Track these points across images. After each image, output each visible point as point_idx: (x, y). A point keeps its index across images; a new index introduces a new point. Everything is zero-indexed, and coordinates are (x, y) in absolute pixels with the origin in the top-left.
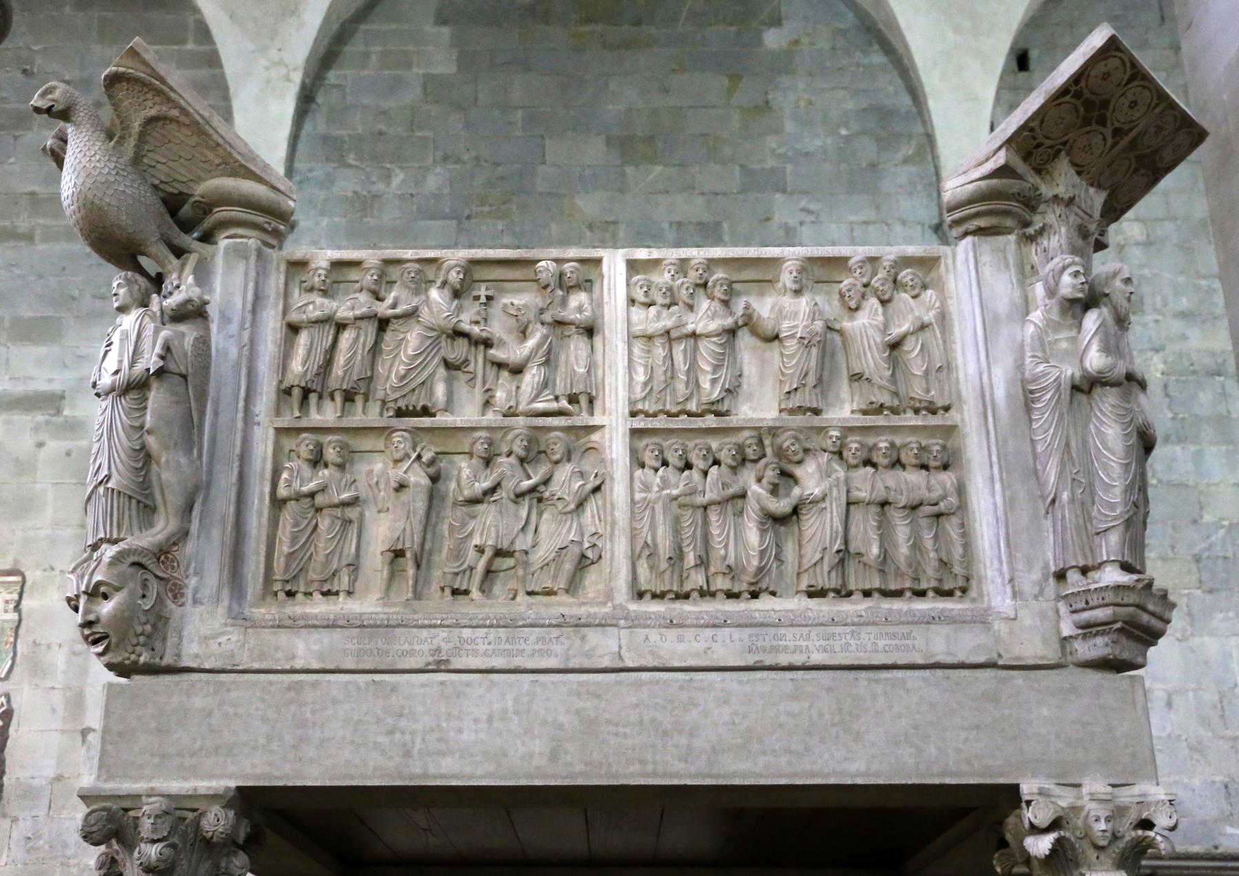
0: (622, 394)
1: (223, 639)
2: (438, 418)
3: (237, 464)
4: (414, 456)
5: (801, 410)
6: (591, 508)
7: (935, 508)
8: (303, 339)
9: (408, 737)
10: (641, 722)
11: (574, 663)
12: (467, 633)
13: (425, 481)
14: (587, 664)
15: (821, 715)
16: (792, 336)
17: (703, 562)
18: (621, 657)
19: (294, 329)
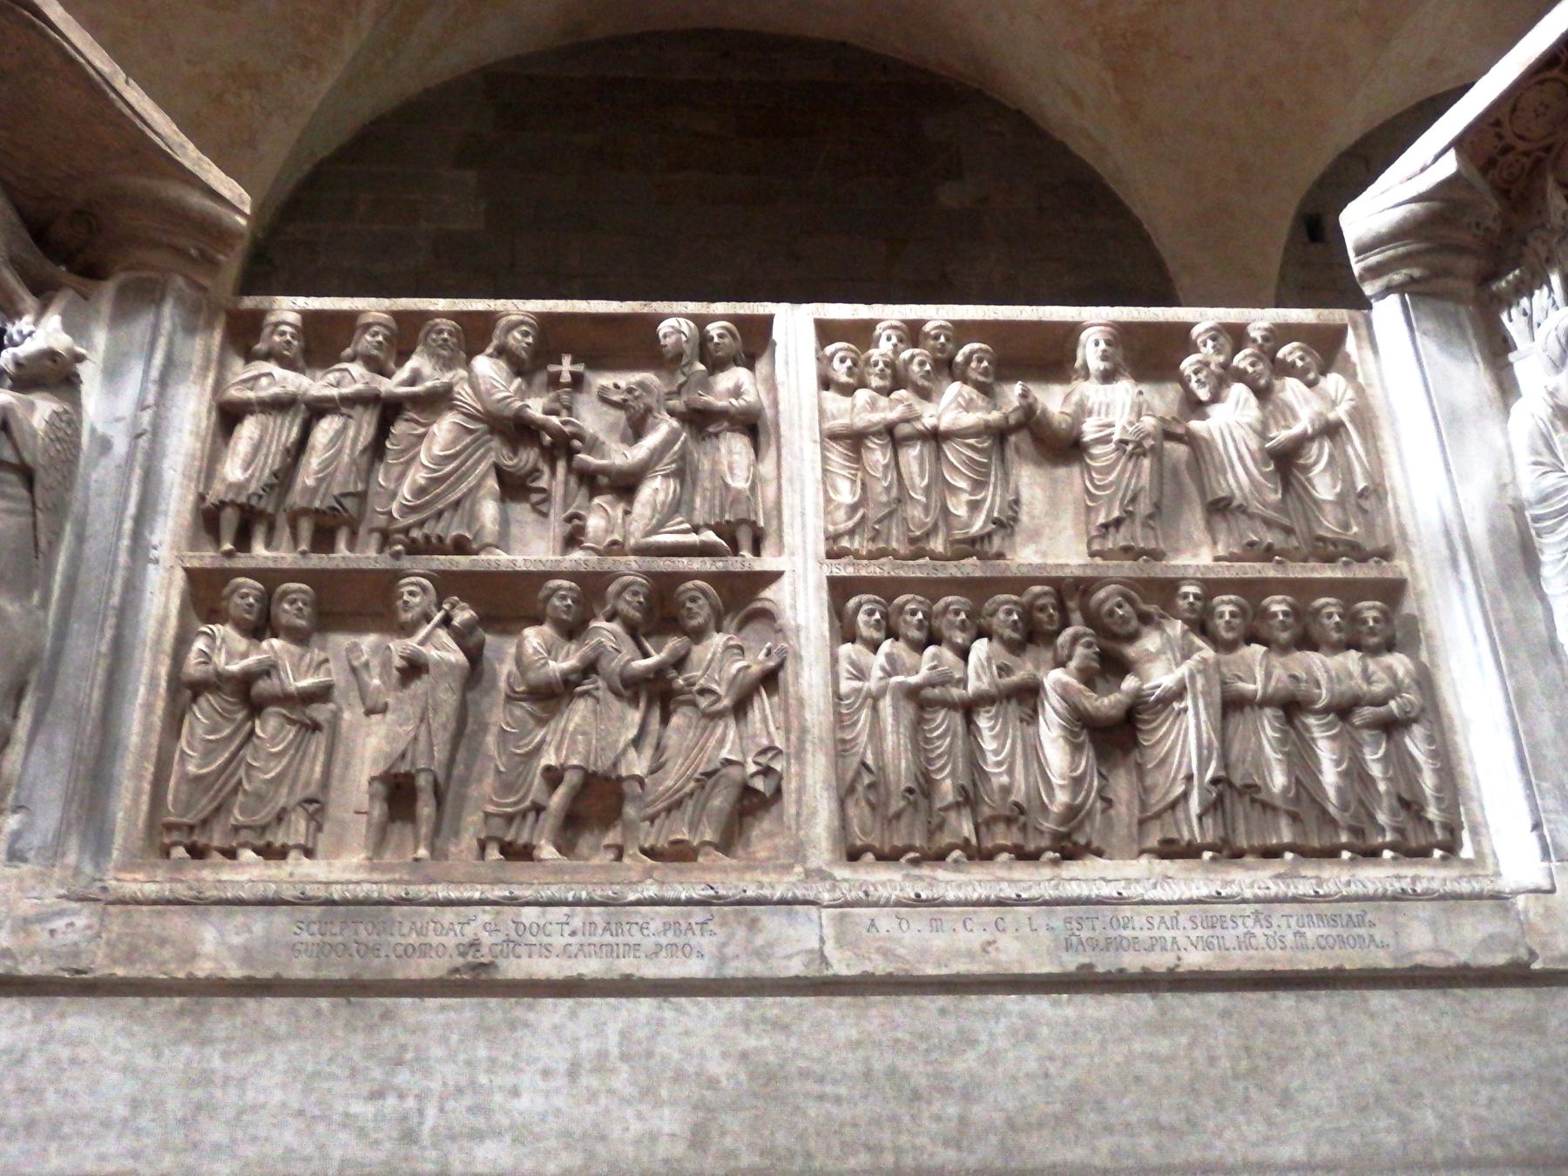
1: (59, 924)
3: (111, 621)
4: (438, 617)
5: (1128, 552)
6: (763, 705)
7: (1382, 709)
8: (248, 430)
9: (411, 1103)
10: (868, 1075)
11: (737, 969)
12: (530, 914)
13: (455, 656)
14: (759, 969)
15: (1212, 1060)
16: (1105, 440)
17: (968, 799)
18: (824, 960)
19: (229, 416)
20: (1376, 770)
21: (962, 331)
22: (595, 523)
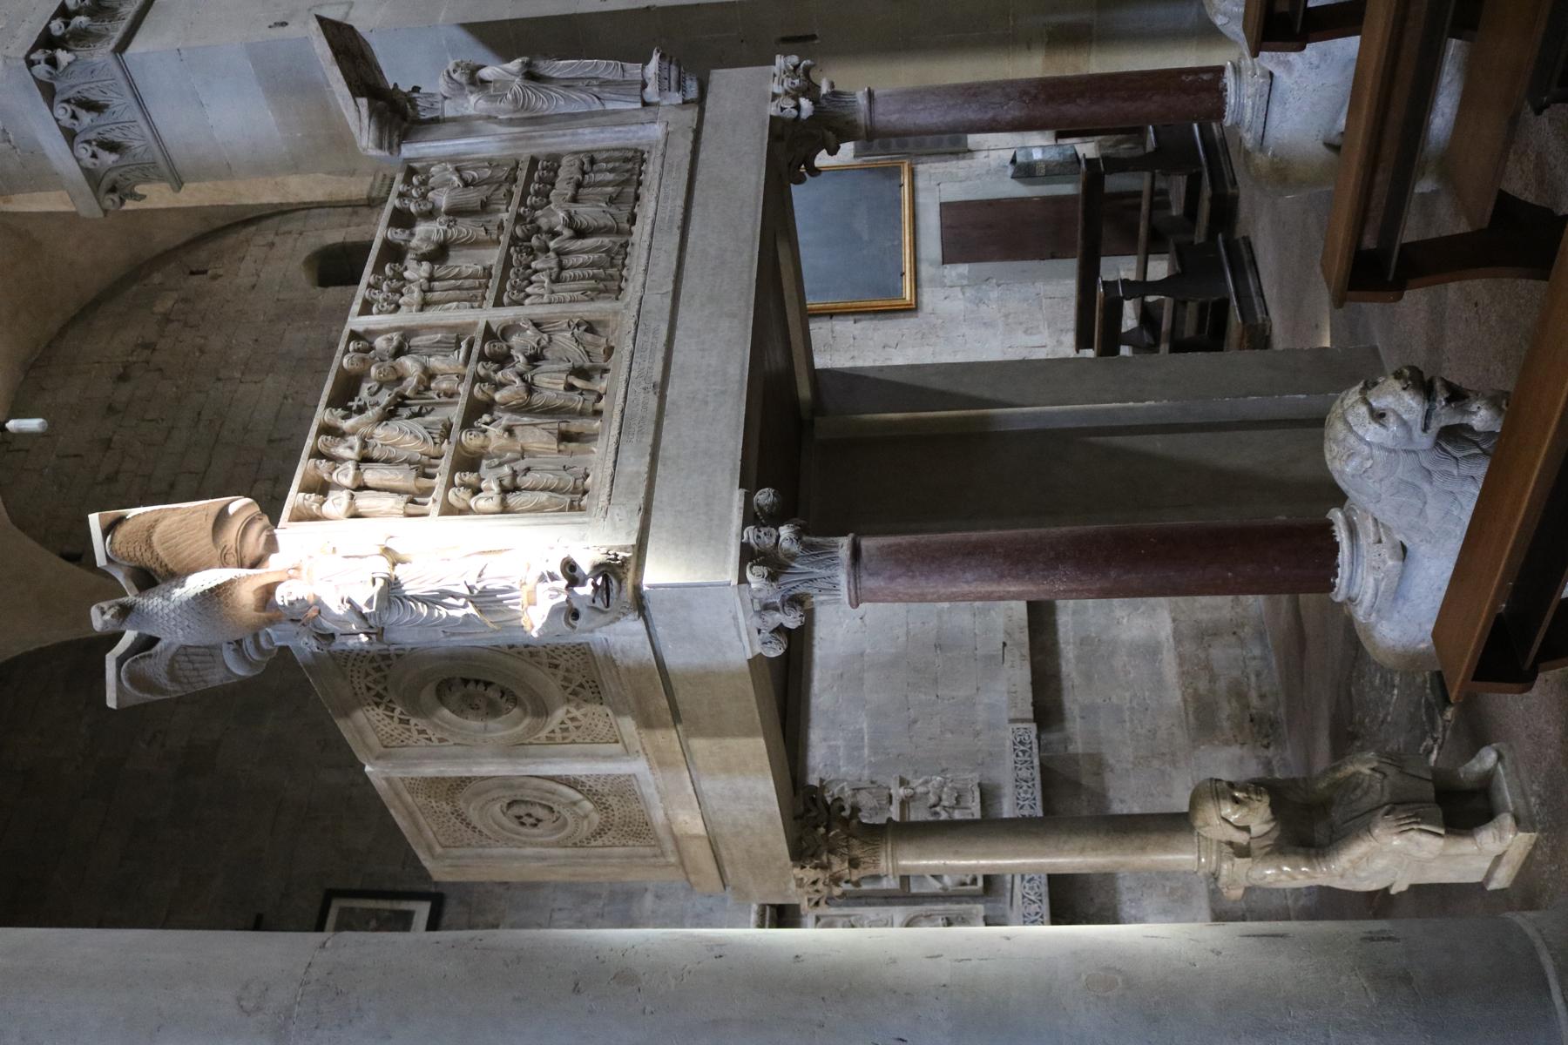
0: (464, 312)
2: (454, 420)
11: (667, 316)
16: (445, 232)
20: (610, 166)
21: (378, 269)
22: (445, 385)
